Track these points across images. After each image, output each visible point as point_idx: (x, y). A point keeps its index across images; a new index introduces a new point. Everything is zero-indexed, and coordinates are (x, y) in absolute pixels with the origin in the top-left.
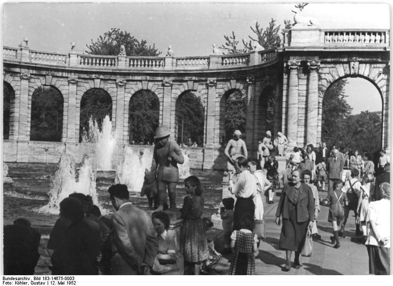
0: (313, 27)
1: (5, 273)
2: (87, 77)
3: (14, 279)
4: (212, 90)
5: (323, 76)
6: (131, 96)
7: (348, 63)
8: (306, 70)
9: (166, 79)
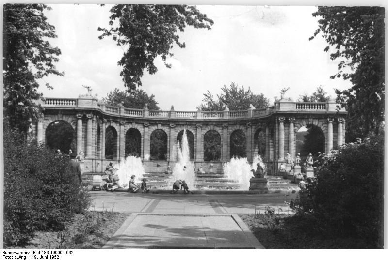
4: (225, 131)
5: (296, 125)
6: (177, 133)
7: (308, 119)
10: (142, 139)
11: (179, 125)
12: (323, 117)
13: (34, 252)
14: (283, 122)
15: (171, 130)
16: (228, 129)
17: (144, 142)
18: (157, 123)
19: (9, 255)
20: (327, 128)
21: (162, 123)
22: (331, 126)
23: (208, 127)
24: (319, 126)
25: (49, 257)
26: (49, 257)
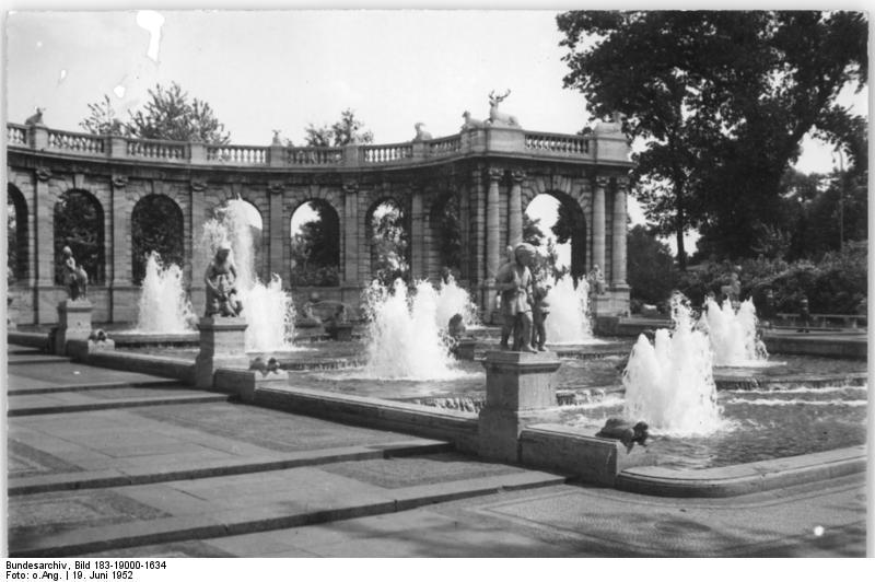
0: (514, 127)
1: (11, 555)
2: (64, 170)
3: (30, 566)
6: (133, 204)
8: (507, 184)
10: (31, 218)
11: (138, 179)
12: (584, 174)
13: (77, 565)
14: (498, 181)
15: (116, 192)
16: (284, 197)
17: (36, 230)
18: (74, 169)
19: (21, 571)
20: (593, 200)
21: (87, 170)
22: (601, 196)
23: (225, 188)
24: (574, 195)
25: (110, 575)
26: (110, 575)
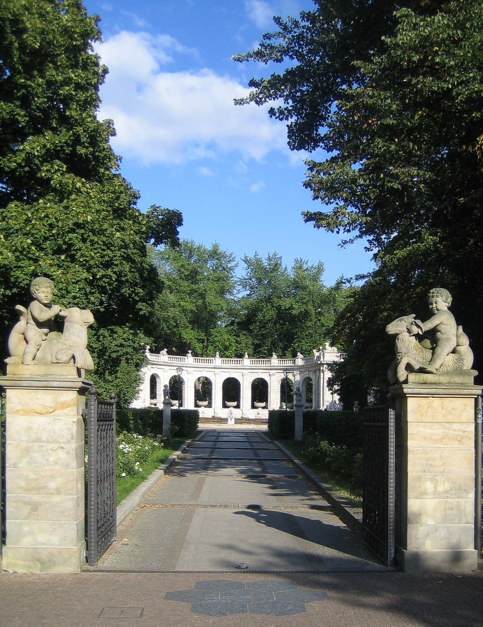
9: (244, 371)
